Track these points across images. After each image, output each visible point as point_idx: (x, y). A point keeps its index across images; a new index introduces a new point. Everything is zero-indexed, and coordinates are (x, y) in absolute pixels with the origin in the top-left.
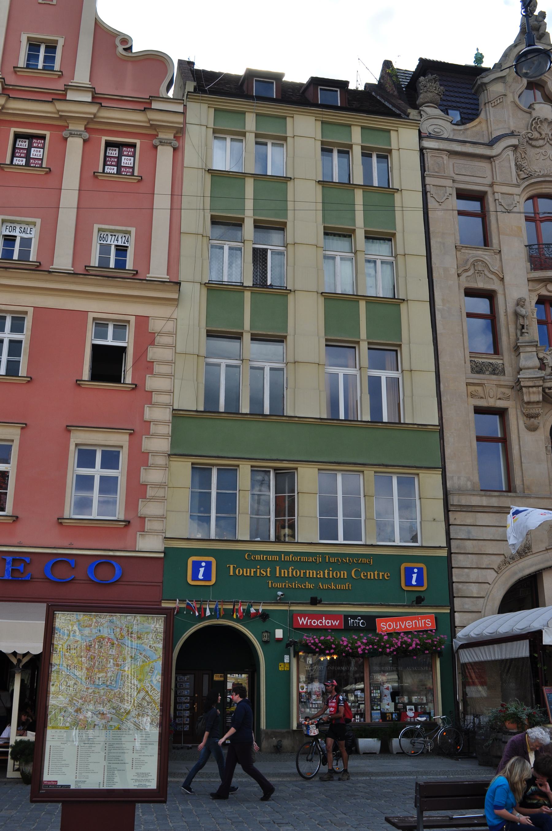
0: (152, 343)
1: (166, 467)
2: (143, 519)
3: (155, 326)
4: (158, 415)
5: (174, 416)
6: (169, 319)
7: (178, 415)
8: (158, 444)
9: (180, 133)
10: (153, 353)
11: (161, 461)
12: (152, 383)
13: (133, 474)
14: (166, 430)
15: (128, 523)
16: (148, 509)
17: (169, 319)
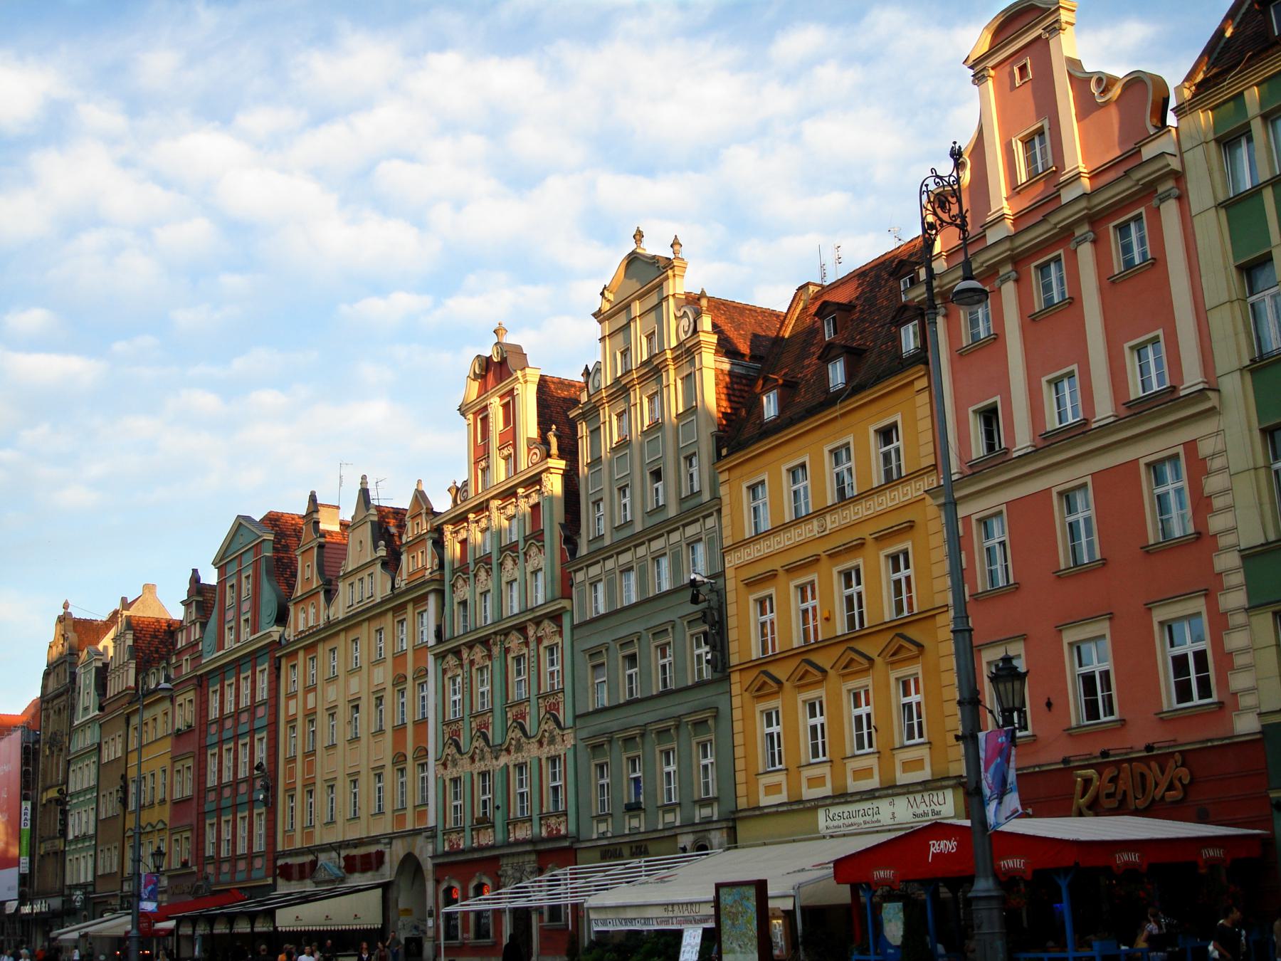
0: (1208, 473)
1: (1246, 626)
2: (1235, 694)
3: (1205, 448)
4: (1227, 561)
5: (1244, 558)
6: (1217, 433)
7: (1249, 556)
8: (1234, 599)
9: (1178, 176)
10: (1213, 484)
11: (1240, 619)
12: (1216, 523)
13: (1217, 642)
14: (1238, 578)
15: (1221, 704)
16: (1238, 681)
17: (1217, 433)
